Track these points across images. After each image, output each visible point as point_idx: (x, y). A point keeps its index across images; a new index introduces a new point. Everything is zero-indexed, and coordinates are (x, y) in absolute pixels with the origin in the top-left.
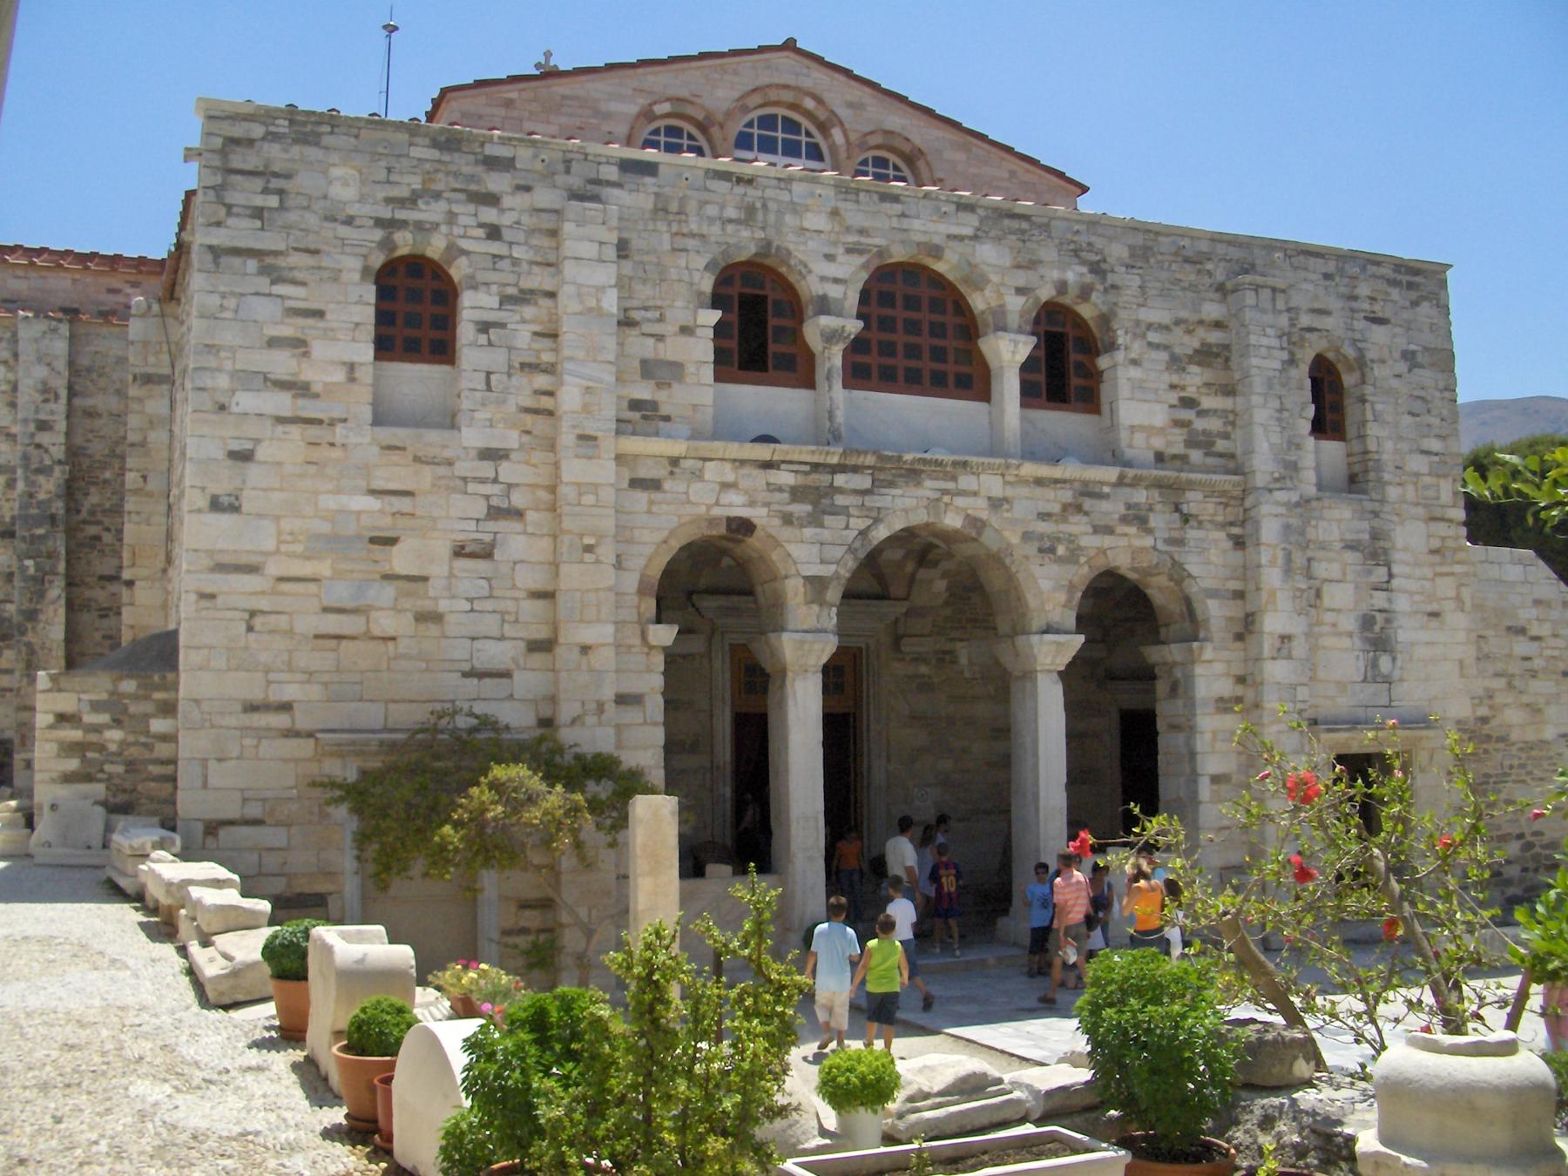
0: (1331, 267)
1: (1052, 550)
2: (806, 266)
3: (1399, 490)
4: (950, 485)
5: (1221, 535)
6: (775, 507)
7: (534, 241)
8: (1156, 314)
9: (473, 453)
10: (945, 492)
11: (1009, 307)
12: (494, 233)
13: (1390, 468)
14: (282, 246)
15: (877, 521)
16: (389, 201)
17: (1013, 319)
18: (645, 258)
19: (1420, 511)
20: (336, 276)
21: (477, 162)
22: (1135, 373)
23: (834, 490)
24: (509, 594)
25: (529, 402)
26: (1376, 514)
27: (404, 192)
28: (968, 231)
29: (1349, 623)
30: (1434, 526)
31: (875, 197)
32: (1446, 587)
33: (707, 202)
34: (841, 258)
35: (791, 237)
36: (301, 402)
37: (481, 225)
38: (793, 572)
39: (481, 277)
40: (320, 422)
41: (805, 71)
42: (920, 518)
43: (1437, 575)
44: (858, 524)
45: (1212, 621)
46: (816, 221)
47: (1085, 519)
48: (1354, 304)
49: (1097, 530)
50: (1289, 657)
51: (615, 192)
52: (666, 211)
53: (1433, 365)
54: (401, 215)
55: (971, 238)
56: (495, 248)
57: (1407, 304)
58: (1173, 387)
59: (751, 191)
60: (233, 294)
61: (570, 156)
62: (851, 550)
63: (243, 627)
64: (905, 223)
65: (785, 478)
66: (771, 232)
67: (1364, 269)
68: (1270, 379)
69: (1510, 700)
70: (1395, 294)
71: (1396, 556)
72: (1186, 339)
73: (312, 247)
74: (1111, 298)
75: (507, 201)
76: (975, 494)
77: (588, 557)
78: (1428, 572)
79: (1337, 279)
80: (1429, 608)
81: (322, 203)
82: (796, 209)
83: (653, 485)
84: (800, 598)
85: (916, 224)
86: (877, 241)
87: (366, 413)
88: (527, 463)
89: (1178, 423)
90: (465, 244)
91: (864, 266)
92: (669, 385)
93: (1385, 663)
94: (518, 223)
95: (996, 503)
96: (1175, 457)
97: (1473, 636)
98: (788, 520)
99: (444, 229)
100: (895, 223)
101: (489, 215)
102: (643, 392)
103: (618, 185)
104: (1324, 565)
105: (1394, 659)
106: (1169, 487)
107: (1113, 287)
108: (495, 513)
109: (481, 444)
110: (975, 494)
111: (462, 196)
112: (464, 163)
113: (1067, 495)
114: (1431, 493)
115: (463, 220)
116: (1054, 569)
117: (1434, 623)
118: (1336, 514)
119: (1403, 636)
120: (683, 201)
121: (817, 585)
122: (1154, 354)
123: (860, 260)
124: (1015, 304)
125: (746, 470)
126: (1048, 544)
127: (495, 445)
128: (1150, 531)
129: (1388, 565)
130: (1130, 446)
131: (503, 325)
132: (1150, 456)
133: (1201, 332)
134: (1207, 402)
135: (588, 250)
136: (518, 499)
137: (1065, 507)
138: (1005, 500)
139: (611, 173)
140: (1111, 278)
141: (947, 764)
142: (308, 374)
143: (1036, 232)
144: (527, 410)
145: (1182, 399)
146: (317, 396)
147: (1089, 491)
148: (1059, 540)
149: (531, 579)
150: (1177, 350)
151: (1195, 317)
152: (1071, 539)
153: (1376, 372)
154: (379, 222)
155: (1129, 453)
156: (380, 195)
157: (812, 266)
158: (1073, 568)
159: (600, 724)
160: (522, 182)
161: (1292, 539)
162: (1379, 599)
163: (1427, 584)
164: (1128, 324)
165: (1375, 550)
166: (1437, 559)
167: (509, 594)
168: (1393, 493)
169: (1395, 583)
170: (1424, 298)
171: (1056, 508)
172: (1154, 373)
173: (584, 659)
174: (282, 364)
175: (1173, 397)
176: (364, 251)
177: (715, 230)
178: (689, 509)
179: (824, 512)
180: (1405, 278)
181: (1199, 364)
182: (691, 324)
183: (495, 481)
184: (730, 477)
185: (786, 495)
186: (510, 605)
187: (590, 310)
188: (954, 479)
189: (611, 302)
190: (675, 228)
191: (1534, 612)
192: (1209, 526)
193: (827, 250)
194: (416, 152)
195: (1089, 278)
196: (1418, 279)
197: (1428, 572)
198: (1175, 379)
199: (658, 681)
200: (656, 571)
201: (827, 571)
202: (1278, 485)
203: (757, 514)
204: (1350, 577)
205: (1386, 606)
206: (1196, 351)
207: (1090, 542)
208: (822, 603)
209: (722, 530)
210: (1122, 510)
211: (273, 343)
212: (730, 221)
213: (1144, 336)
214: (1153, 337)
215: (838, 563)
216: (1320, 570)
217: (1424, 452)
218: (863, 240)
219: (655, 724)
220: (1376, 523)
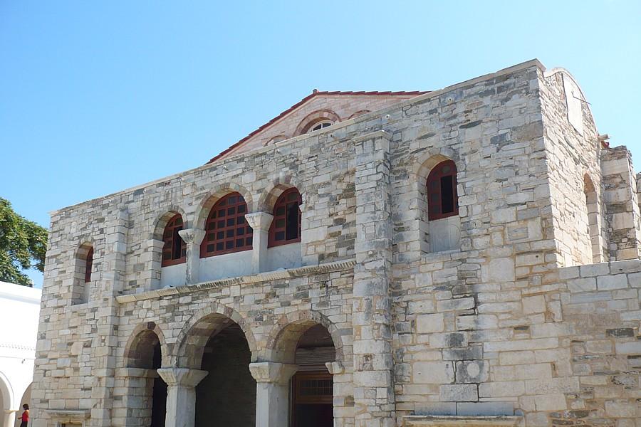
0: (435, 103)
1: (261, 319)
3: (487, 239)
4: (219, 294)
13: (479, 224)
15: (192, 316)
17: (255, 206)
19: (507, 250)
26: (463, 261)
27: (84, 225)
28: (240, 171)
29: (439, 341)
32: (536, 304)
41: (325, 101)
42: (209, 311)
43: (523, 296)
44: (186, 318)
45: (344, 349)
46: (187, 191)
47: (276, 299)
48: (452, 122)
49: (282, 306)
50: (372, 369)
53: (520, 139)
57: (498, 102)
58: (331, 215)
59: (169, 187)
63: (42, 375)
65: (165, 303)
67: (461, 93)
68: (368, 194)
69: (613, 395)
70: (487, 100)
71: (482, 288)
72: (339, 184)
76: (229, 296)
78: (516, 295)
79: (439, 111)
80: (516, 324)
84: (166, 354)
85: (221, 177)
86: (206, 191)
89: (332, 235)
93: (473, 369)
95: (237, 299)
96: (330, 255)
97: (567, 342)
103: (133, 201)
104: (419, 303)
105: (481, 366)
106: (320, 273)
107: (300, 172)
110: (229, 296)
112: (98, 209)
113: (268, 289)
114: (520, 233)
116: (261, 329)
117: (522, 335)
118: (430, 267)
119: (488, 347)
121: (171, 346)
123: (200, 201)
128: (309, 301)
132: (316, 257)
138: (241, 296)
145: (335, 221)
147: (279, 285)
150: (334, 194)
151: (344, 171)
153: (467, 161)
155: (305, 259)
162: (467, 322)
163: (514, 306)
166: (525, 283)
168: (479, 243)
169: (481, 308)
170: (513, 93)
171: (263, 297)
180: (495, 87)
183: (94, 319)
192: (343, 291)
196: (507, 82)
197: (516, 295)
198: (332, 210)
203: (156, 320)
204: (438, 310)
205: (473, 326)
207: (279, 311)
210: (294, 290)
212: (162, 202)
214: (321, 191)
216: (414, 307)
217: (509, 205)
219: (124, 408)
220: (463, 267)
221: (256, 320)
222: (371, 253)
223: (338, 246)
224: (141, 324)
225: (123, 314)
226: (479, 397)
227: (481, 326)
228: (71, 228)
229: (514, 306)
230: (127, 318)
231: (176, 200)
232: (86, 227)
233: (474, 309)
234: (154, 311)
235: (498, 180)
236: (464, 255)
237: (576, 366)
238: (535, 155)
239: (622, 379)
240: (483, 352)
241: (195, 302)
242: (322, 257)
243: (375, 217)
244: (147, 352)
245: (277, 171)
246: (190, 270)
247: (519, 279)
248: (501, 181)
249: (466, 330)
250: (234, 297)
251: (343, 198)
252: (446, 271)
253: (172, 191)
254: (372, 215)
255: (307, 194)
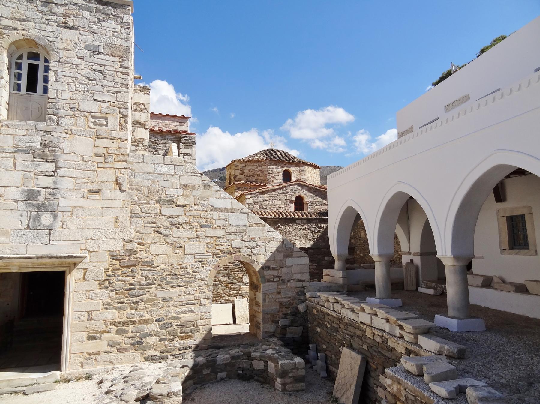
29: (15, 193)
30: (100, 142)
48: (50, 17)
70: (87, 14)
71: (63, 157)
80: (90, 187)
93: (46, 219)
105: (55, 217)
117: (94, 196)
119: (63, 203)
129: (56, 161)
165: (47, 152)
166: (102, 160)
168: (65, 121)
191: (181, 192)
205: (52, 185)
217: (95, 100)
220: (47, 137)
226: (50, 241)
227: (59, 186)
229: (90, 174)
233: (54, 172)
235: (87, 78)
236: (49, 129)
237: (134, 220)
238: (121, 70)
239: (162, 230)
240: (58, 206)
247: (96, 155)
248: (90, 80)
249: (44, 188)
252: (28, 138)
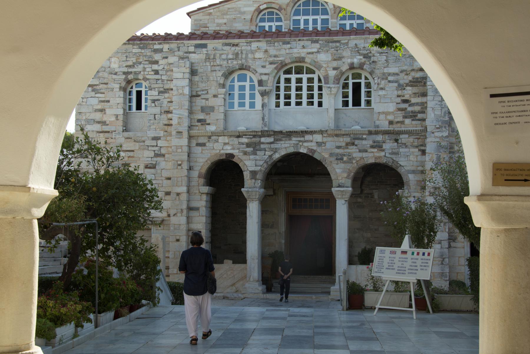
1: (342, 159)
2: (255, 71)
5: (417, 150)
6: (241, 149)
7: (168, 73)
8: (393, 69)
9: (150, 138)
10: (300, 141)
11: (330, 75)
12: (157, 72)
14: (98, 83)
15: (275, 152)
16: (126, 66)
18: (203, 75)
20: (112, 90)
21: (152, 51)
22: (381, 93)
23: (260, 143)
24: (160, 178)
25: (166, 122)
27: (130, 63)
31: (281, 43)
33: (222, 54)
34: (267, 67)
35: (250, 61)
36: (104, 127)
37: (153, 71)
38: (246, 169)
39: (153, 86)
40: (109, 132)
42: (291, 150)
44: (268, 153)
45: (410, 182)
47: (355, 147)
49: (360, 151)
51: (193, 55)
52: (209, 58)
54: (130, 70)
55: (316, 53)
56: (157, 77)
58: (398, 96)
59: (237, 48)
60: (85, 98)
61: (179, 45)
62: (266, 162)
64: (291, 51)
65: (244, 140)
66: (244, 61)
72: (406, 77)
73: (106, 82)
74: (372, 66)
75: (160, 63)
77: (179, 167)
81: (108, 69)
82: (253, 52)
83: (204, 145)
85: (295, 50)
86: (281, 59)
87: (121, 129)
88: (166, 140)
90: (148, 77)
91: (275, 68)
92: (210, 114)
94: (164, 68)
95: (319, 144)
96: (398, 122)
98: (245, 153)
99: (142, 73)
100: (287, 51)
101: (155, 67)
102: (201, 116)
103: (194, 53)
107: (373, 62)
108: (156, 155)
109: (153, 136)
111: (147, 62)
112: (148, 52)
113: (348, 139)
115: (148, 70)
116: (342, 165)
120: (215, 55)
121: (254, 174)
122: (391, 84)
123: (275, 66)
124: (332, 73)
125: (232, 139)
126: (340, 157)
127: (156, 136)
128: (383, 150)
130: (378, 120)
131: (158, 100)
132: (387, 123)
133: (413, 74)
134: (414, 100)
135: (180, 75)
136: (163, 151)
137: (347, 144)
138: (323, 143)
139: (192, 49)
140: (373, 59)
141: (369, 235)
142: (105, 119)
143: (342, 46)
144: (166, 125)
146: (108, 125)
148: (344, 155)
149: (165, 174)
150: (401, 82)
152: (349, 155)
154: (124, 73)
156: (124, 65)
157: (257, 70)
158: (350, 165)
159: (182, 216)
160: (165, 56)
161: (441, 151)
164: (379, 75)
167: (160, 178)
171: (344, 144)
172: (391, 90)
173: (177, 197)
174: (98, 116)
175: (399, 100)
176: (120, 82)
177: (225, 62)
178: (214, 152)
179: (257, 150)
181: (412, 86)
182: (216, 94)
183: (157, 146)
184: (227, 141)
185: (245, 146)
186: (161, 182)
187: (181, 94)
188: (304, 137)
189: (187, 91)
190: (212, 64)
193: (263, 64)
194: (134, 51)
195: (363, 60)
198: (400, 93)
199: (203, 203)
200: (204, 171)
201: (259, 168)
202: (438, 130)
203: (235, 152)
206: (410, 81)
207: (357, 155)
208: (256, 179)
209: (224, 157)
211: (96, 110)
212: (230, 59)
213: (387, 79)
214: (390, 78)
215: (261, 166)
218: (275, 59)
219: (202, 216)
221: (337, 159)
222: (438, 126)
223: (405, 117)
224: (216, 155)
225: (194, 145)
228: (110, 63)
230: (200, 148)
231: (246, 61)
232: (134, 66)
234: (232, 145)
241: (277, 142)
242: (391, 123)
243: (442, 105)
244: (224, 176)
245: (352, 57)
246: (266, 118)
250: (317, 142)
251: (409, 86)
253: (242, 53)
254: (440, 103)
255: (379, 78)
